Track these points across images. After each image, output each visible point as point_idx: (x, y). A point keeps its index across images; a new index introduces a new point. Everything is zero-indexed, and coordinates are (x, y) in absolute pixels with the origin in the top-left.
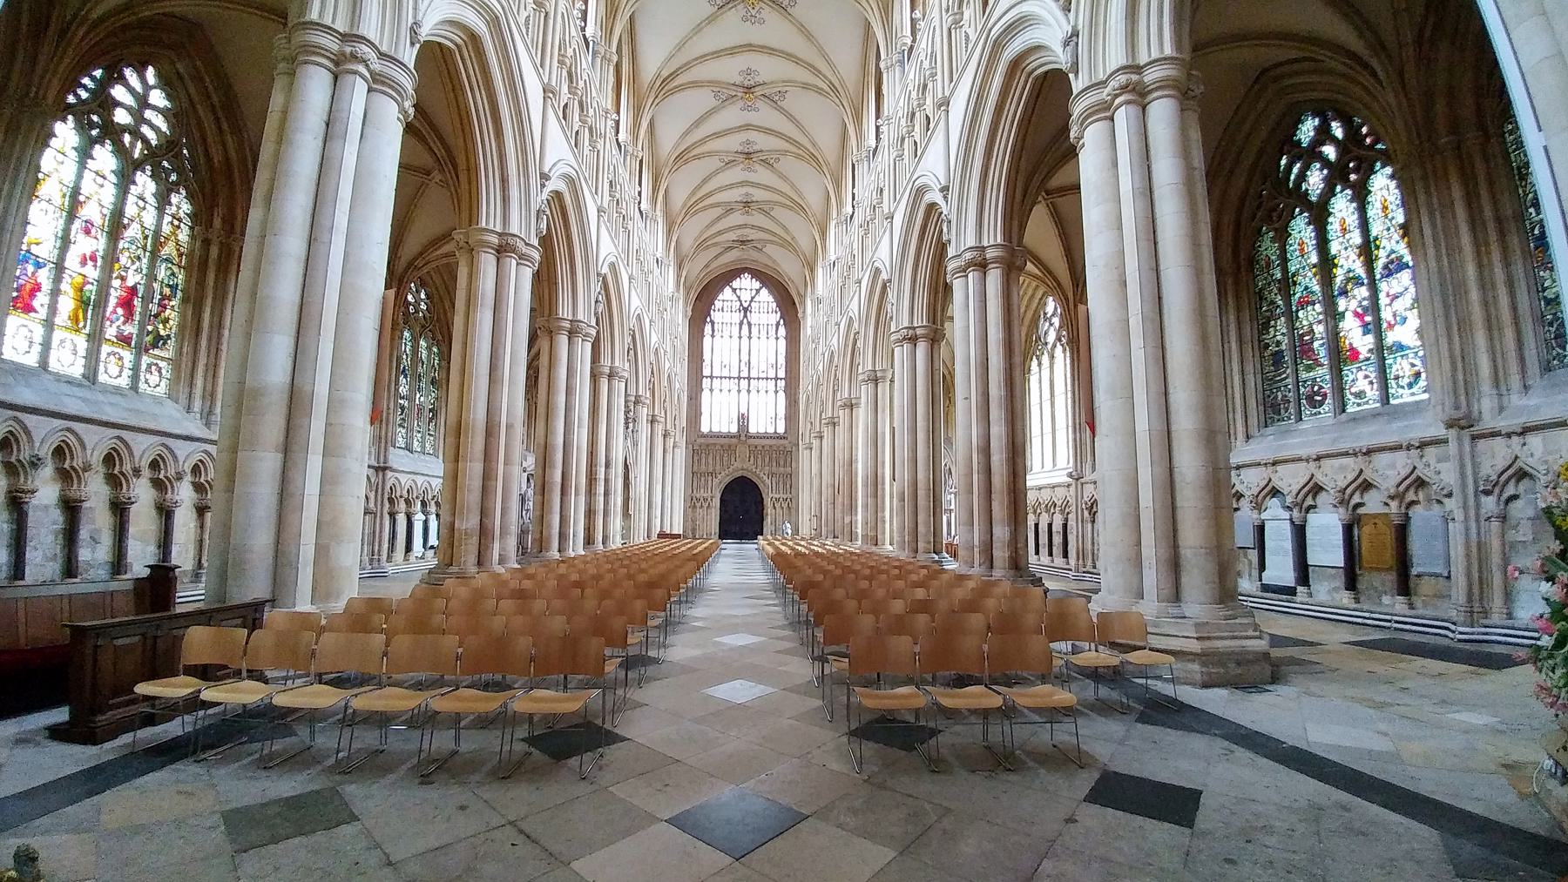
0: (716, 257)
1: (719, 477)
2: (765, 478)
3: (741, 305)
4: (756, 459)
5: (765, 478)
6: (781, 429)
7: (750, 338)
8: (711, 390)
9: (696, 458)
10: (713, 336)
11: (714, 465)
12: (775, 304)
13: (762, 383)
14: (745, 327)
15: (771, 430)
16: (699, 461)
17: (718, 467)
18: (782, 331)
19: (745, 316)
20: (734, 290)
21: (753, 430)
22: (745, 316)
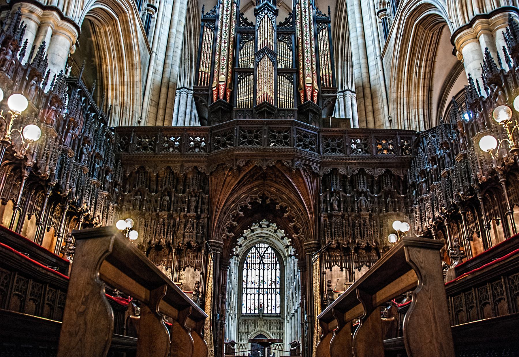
0: (250, 242)
1: (250, 334)
2: (271, 335)
3: (260, 255)
4: (267, 326)
5: (271, 335)
6: (278, 311)
7: (264, 270)
8: (247, 294)
9: (240, 326)
10: (247, 270)
11: (248, 329)
12: (275, 254)
13: (270, 290)
14: (262, 265)
15: (273, 312)
16: (242, 327)
17: (250, 330)
18: (278, 267)
19: (262, 260)
20: (257, 248)
21: (265, 312)
22: (262, 260)
